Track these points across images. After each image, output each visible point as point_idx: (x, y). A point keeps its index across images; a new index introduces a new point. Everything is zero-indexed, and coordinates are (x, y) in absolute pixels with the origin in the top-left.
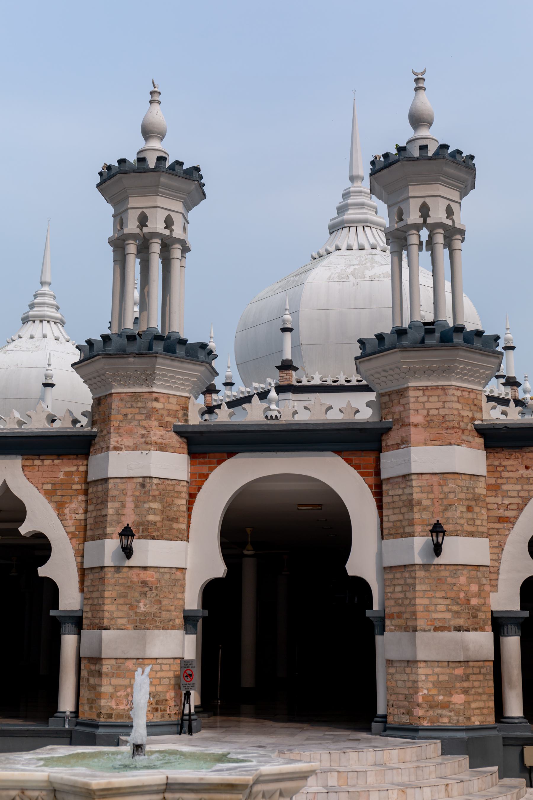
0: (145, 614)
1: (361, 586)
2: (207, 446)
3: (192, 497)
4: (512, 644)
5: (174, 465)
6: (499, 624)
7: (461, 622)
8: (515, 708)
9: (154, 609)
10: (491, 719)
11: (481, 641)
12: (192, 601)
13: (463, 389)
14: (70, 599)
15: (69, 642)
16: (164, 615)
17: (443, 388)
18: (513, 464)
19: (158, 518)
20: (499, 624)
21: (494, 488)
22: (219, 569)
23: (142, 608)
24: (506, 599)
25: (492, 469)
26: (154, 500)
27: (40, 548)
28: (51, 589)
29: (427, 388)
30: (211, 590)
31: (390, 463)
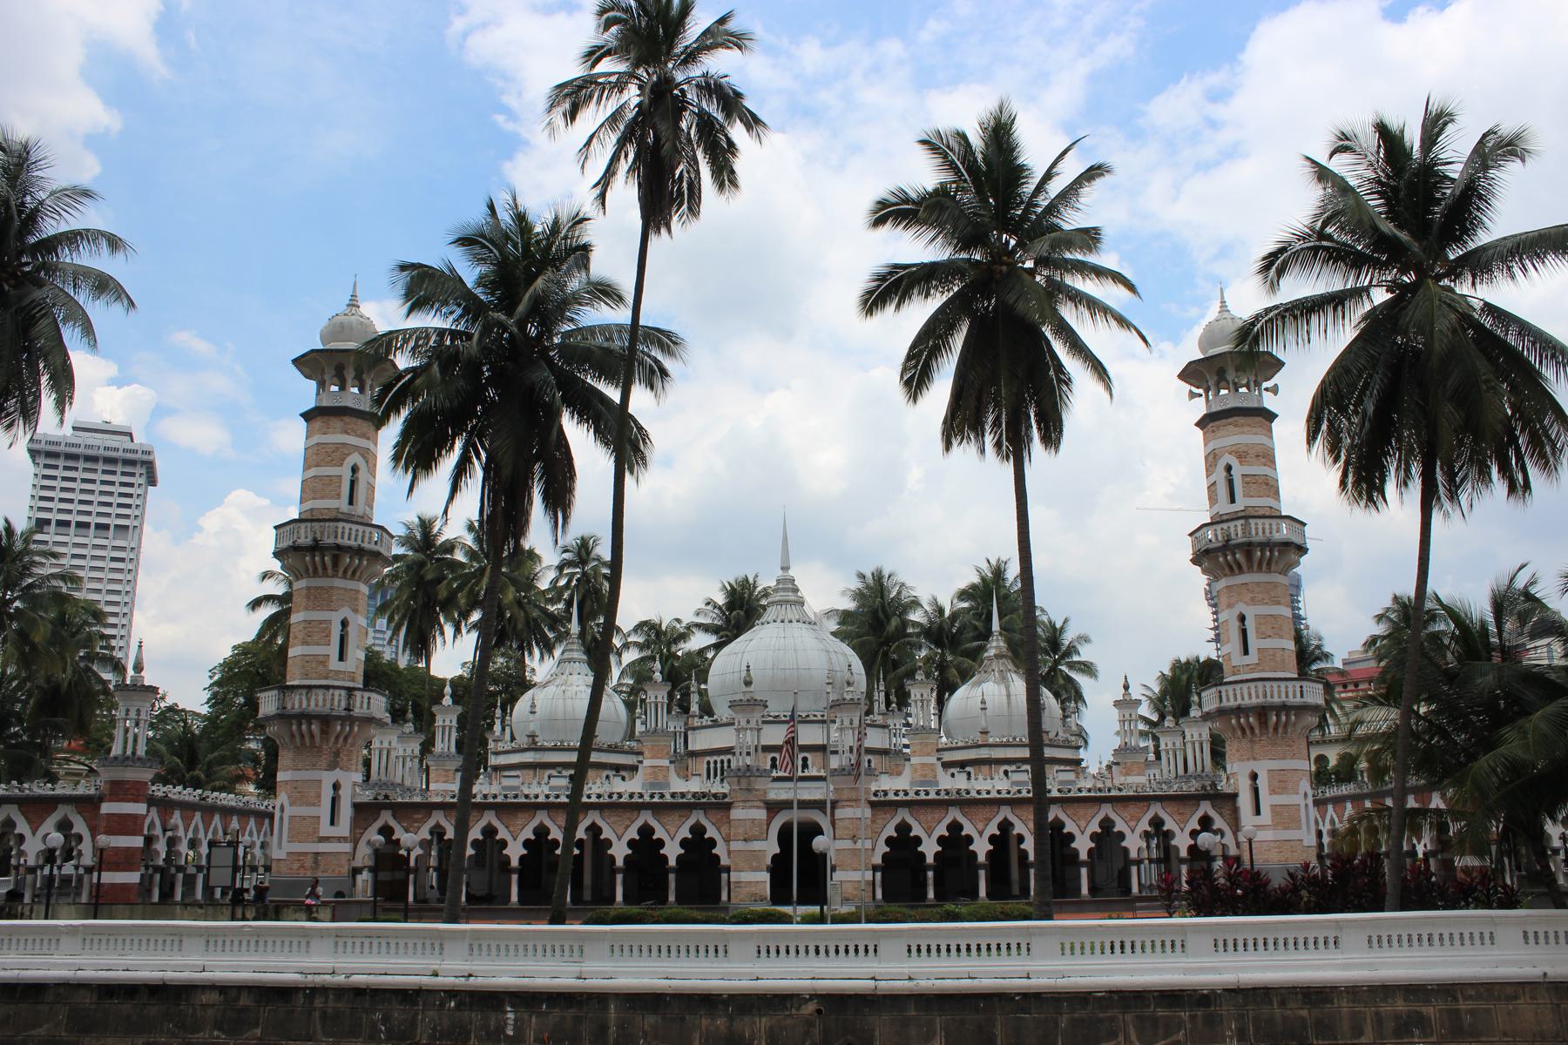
3: (768, 825)
4: (879, 875)
5: (761, 814)
6: (875, 868)
8: (879, 895)
11: (869, 875)
12: (769, 862)
14: (724, 861)
15: (724, 876)
20: (875, 868)
21: (873, 821)
22: (778, 850)
24: (878, 860)
27: (712, 843)
28: (717, 857)
30: (775, 857)
31: (839, 813)
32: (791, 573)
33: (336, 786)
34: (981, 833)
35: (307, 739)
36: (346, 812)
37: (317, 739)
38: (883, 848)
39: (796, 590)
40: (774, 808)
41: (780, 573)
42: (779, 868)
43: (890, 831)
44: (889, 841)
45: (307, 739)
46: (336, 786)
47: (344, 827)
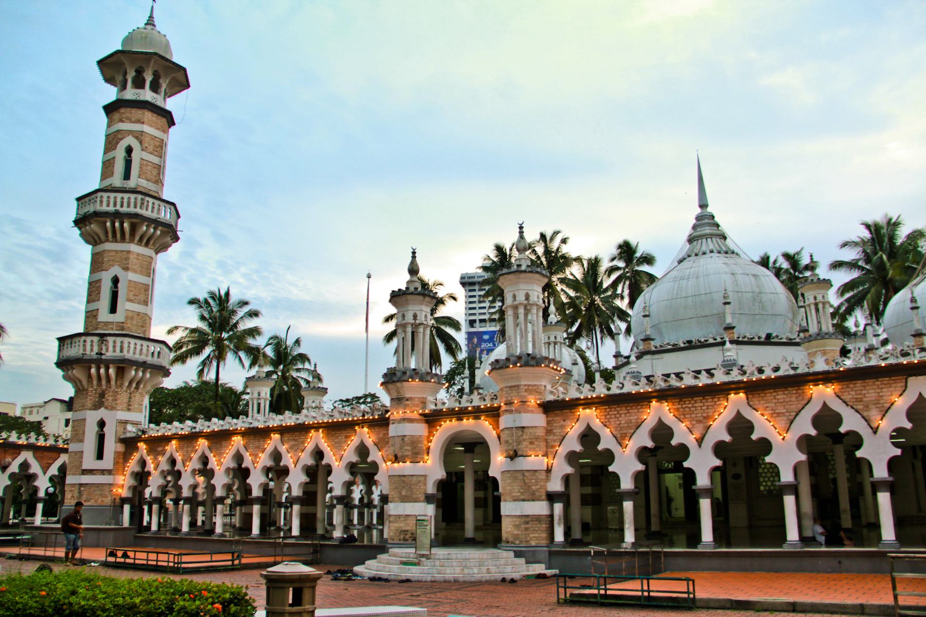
0: (406, 496)
1: (494, 480)
2: (432, 419)
4: (558, 507)
5: (420, 429)
7: (523, 497)
8: (559, 536)
9: (409, 493)
10: (544, 542)
12: (431, 489)
13: (529, 386)
16: (415, 496)
17: (518, 386)
18: (558, 420)
19: (409, 453)
20: (552, 498)
23: (404, 493)
24: (556, 485)
25: (548, 423)
26: (408, 445)
29: (511, 387)
32: (709, 209)
33: (102, 424)
34: (700, 441)
35: (104, 382)
36: (111, 447)
37: (113, 383)
38: (562, 468)
39: (718, 226)
40: (432, 419)
41: (699, 211)
42: (447, 497)
43: (573, 444)
44: (572, 457)
45: (104, 382)
46: (102, 424)
47: (108, 462)
